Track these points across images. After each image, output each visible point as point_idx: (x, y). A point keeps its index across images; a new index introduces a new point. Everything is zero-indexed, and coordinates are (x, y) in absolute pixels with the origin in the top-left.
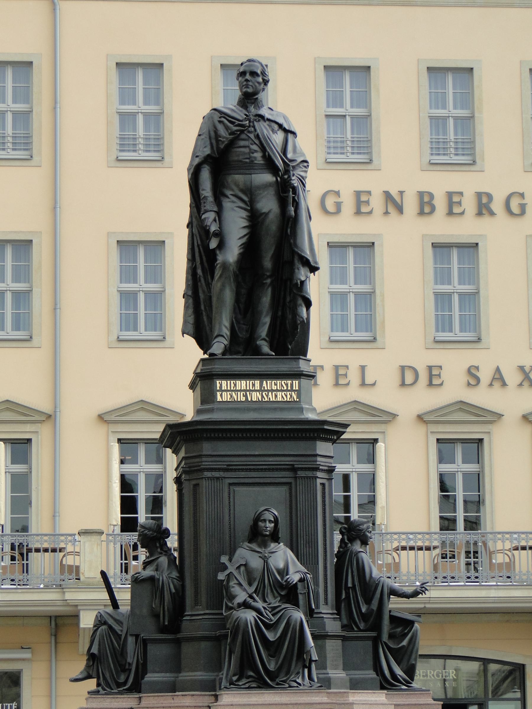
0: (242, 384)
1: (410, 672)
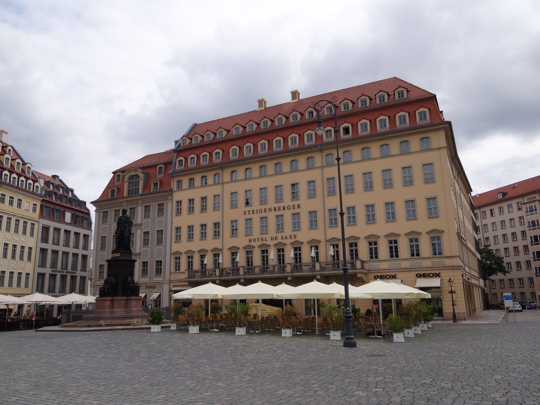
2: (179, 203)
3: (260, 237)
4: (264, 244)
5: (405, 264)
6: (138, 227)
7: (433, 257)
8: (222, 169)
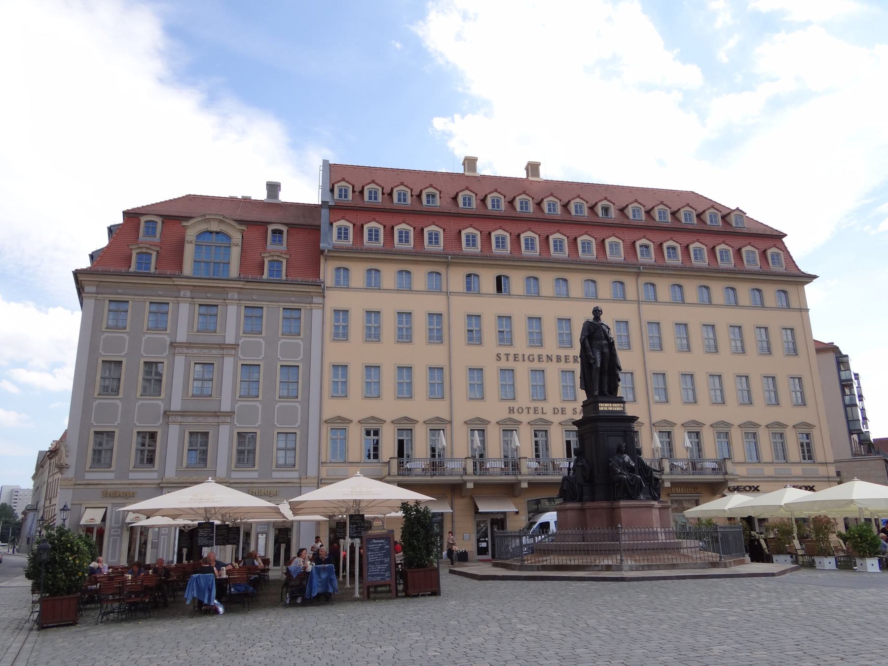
0: (606, 405)
1: (659, 495)
2: (342, 313)
3: (533, 405)
4: (541, 420)
5: (769, 471)
6: (225, 352)
7: (800, 463)
8: (448, 264)
